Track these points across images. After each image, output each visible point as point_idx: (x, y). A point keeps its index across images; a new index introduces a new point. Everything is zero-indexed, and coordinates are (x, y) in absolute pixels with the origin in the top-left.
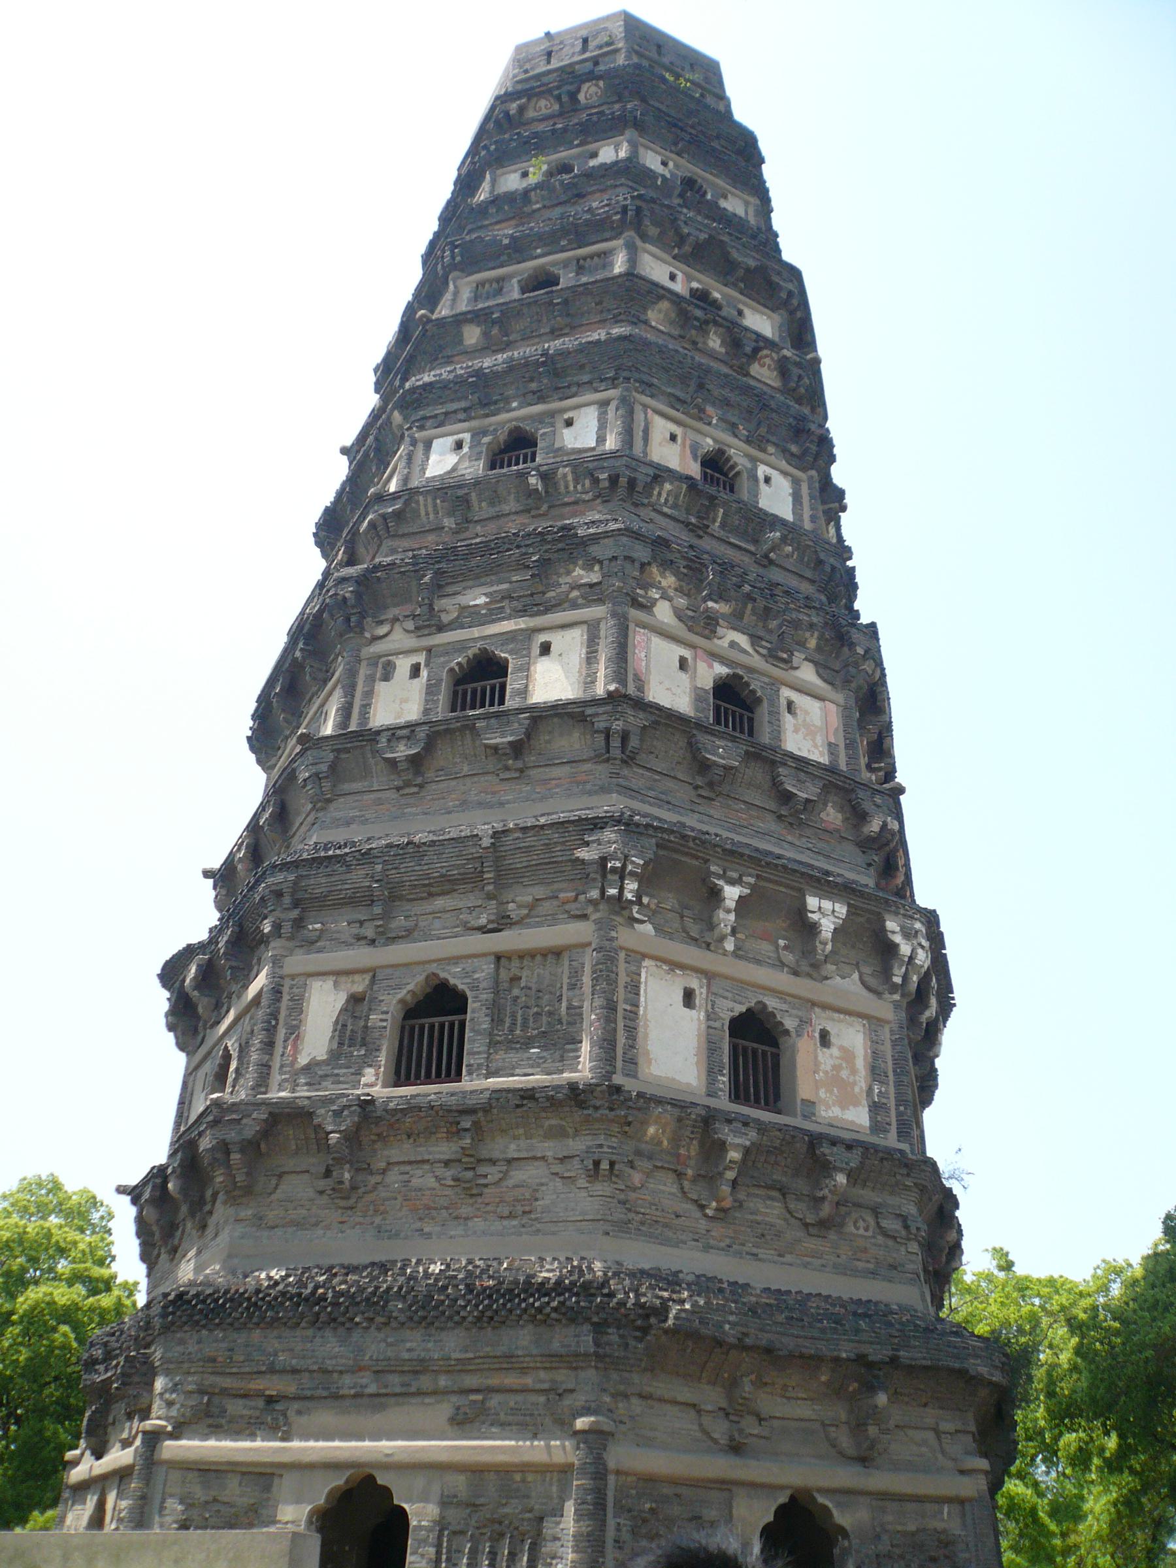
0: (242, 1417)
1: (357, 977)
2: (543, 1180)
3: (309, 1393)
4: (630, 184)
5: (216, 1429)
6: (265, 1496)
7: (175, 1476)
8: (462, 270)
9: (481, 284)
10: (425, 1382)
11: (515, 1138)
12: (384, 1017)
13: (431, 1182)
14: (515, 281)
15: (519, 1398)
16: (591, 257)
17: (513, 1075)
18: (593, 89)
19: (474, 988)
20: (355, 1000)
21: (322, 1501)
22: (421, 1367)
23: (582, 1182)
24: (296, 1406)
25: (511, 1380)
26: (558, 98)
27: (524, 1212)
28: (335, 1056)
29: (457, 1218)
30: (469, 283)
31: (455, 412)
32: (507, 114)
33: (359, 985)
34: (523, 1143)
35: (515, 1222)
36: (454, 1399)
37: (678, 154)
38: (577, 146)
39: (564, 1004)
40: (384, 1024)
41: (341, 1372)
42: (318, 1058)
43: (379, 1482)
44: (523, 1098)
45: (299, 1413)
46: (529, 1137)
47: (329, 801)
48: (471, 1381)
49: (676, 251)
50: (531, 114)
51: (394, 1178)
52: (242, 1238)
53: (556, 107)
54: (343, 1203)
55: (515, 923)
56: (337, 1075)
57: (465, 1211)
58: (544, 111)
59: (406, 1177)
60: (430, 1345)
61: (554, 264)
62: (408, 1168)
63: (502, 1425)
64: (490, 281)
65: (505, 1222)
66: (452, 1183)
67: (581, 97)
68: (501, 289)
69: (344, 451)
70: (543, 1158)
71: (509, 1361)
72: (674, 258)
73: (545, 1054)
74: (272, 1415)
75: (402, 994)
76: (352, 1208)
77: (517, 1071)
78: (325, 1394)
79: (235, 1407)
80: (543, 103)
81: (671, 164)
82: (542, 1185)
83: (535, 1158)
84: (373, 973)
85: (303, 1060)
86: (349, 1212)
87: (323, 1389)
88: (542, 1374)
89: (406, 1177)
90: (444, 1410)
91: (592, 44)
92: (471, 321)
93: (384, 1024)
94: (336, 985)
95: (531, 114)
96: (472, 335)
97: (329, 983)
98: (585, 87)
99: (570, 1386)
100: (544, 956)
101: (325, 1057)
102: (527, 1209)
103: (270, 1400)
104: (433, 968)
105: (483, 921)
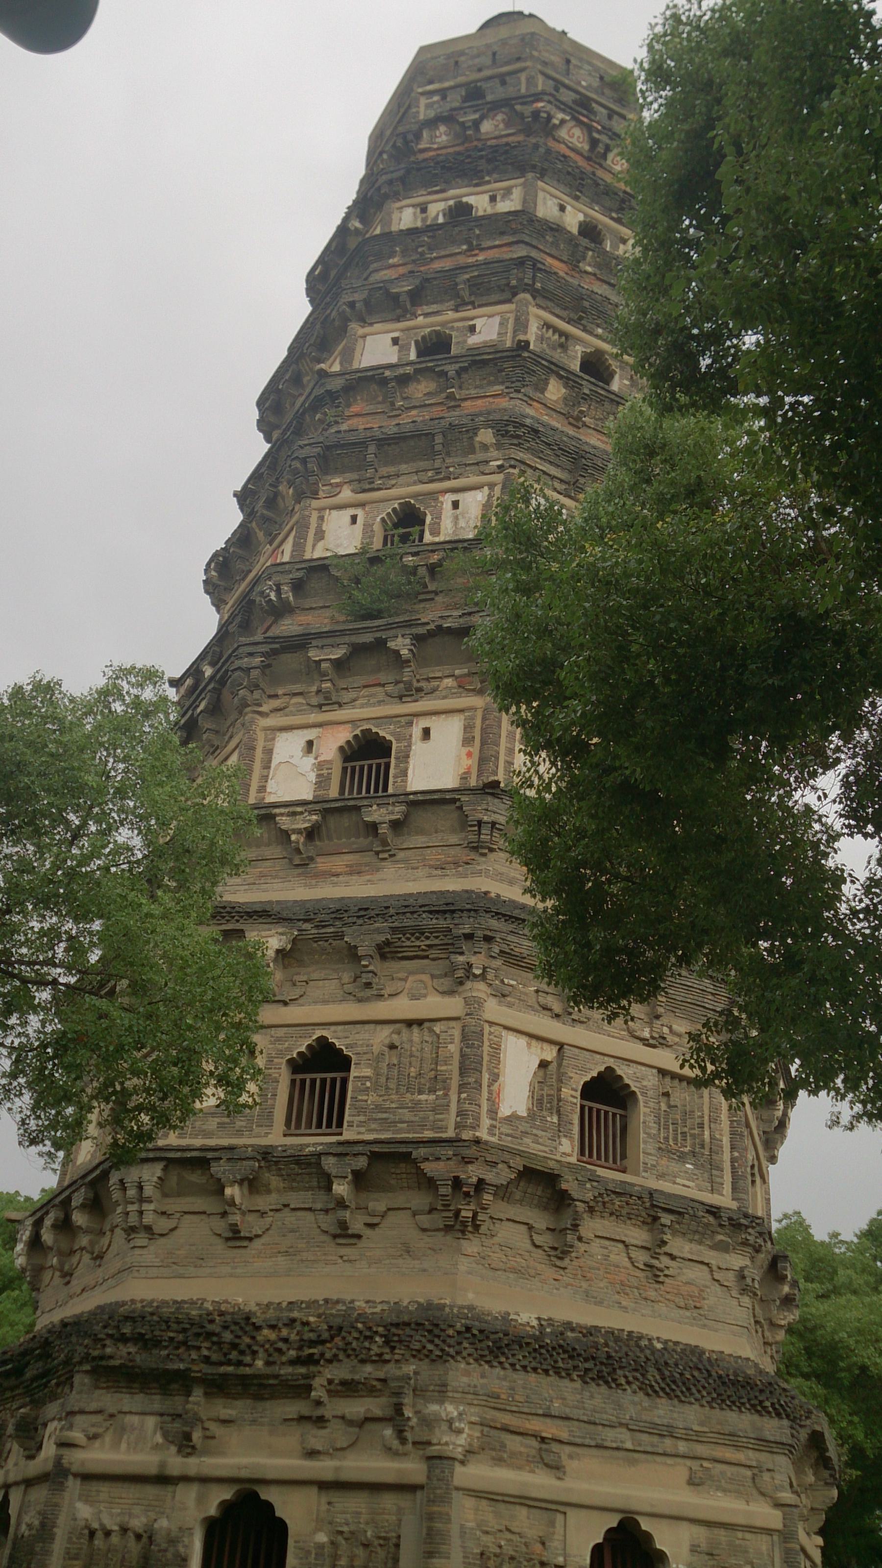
0: (521, 1453)
1: (546, 1046)
2: (708, 1283)
3: (579, 1441)
5: (499, 1461)
6: (551, 1530)
7: (469, 1503)
8: (534, 298)
10: (668, 1444)
11: (691, 1241)
12: (573, 1093)
13: (626, 1262)
15: (734, 1469)
17: (674, 1183)
19: (644, 1094)
20: (543, 1065)
21: (658, 1547)
22: (669, 1432)
23: (735, 1293)
24: (568, 1449)
25: (729, 1454)
26: (594, 143)
27: (695, 1307)
28: (532, 1115)
29: (646, 1299)
31: (553, 478)
33: (550, 1053)
34: (695, 1247)
35: (688, 1314)
36: (689, 1463)
38: (612, 218)
39: (707, 1133)
40: (575, 1101)
41: (603, 1425)
42: (519, 1114)
43: (644, 1527)
44: (708, 1212)
45: (571, 1457)
46: (700, 1243)
47: (491, 850)
48: (701, 1450)
51: (596, 1247)
52: (470, 1273)
53: (586, 147)
54: (559, 1263)
55: (667, 1046)
56: (536, 1135)
57: (652, 1294)
58: (574, 140)
59: (605, 1252)
60: (675, 1415)
62: (607, 1243)
63: (724, 1491)
64: (556, 330)
65: (682, 1312)
66: (642, 1267)
70: (707, 1264)
71: (732, 1439)
73: (696, 1172)
74: (547, 1454)
75: (588, 1078)
76: (564, 1268)
77: (678, 1180)
78: (593, 1443)
79: (514, 1443)
80: (577, 132)
82: (707, 1287)
83: (702, 1263)
84: (561, 1046)
85: (505, 1111)
86: (562, 1272)
87: (591, 1438)
88: (751, 1453)
89: (605, 1252)
90: (680, 1471)
92: (561, 377)
93: (575, 1101)
94: (529, 1045)
95: (563, 133)
97: (523, 1041)
99: (771, 1467)
100: (688, 1083)
101: (525, 1115)
102: (698, 1305)
103: (543, 1440)
104: (611, 1062)
105: (646, 1034)
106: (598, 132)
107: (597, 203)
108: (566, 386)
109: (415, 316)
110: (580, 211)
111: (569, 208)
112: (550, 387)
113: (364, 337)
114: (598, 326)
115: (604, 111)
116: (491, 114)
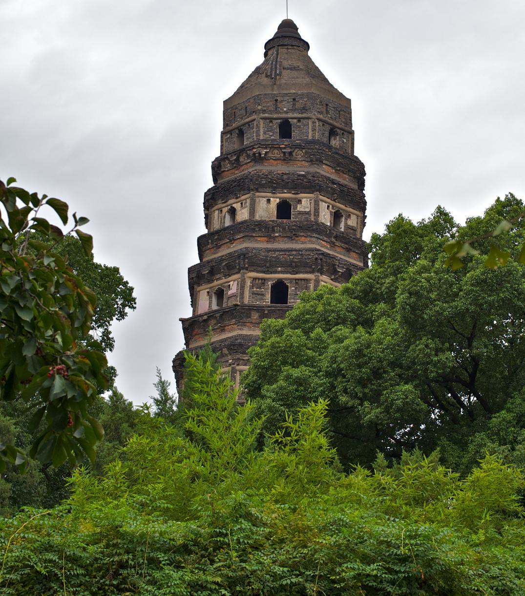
4: (317, 236)
9: (255, 279)
14: (269, 283)
16: (301, 280)
18: (301, 152)
30: (250, 277)
32: (260, 154)
37: (334, 200)
38: (293, 194)
49: (333, 277)
50: (270, 155)
58: (276, 155)
61: (286, 279)
67: (294, 154)
68: (263, 284)
69: (182, 320)
72: (332, 279)
80: (276, 151)
81: (331, 206)
91: (298, 106)
96: (255, 316)
98: (296, 151)
106: (284, 148)
107: (285, 189)
108: (258, 312)
109: (213, 281)
110: (277, 198)
111: (272, 199)
112: (252, 315)
113: (199, 291)
114: (278, 267)
115: (295, 121)
116: (241, 154)
